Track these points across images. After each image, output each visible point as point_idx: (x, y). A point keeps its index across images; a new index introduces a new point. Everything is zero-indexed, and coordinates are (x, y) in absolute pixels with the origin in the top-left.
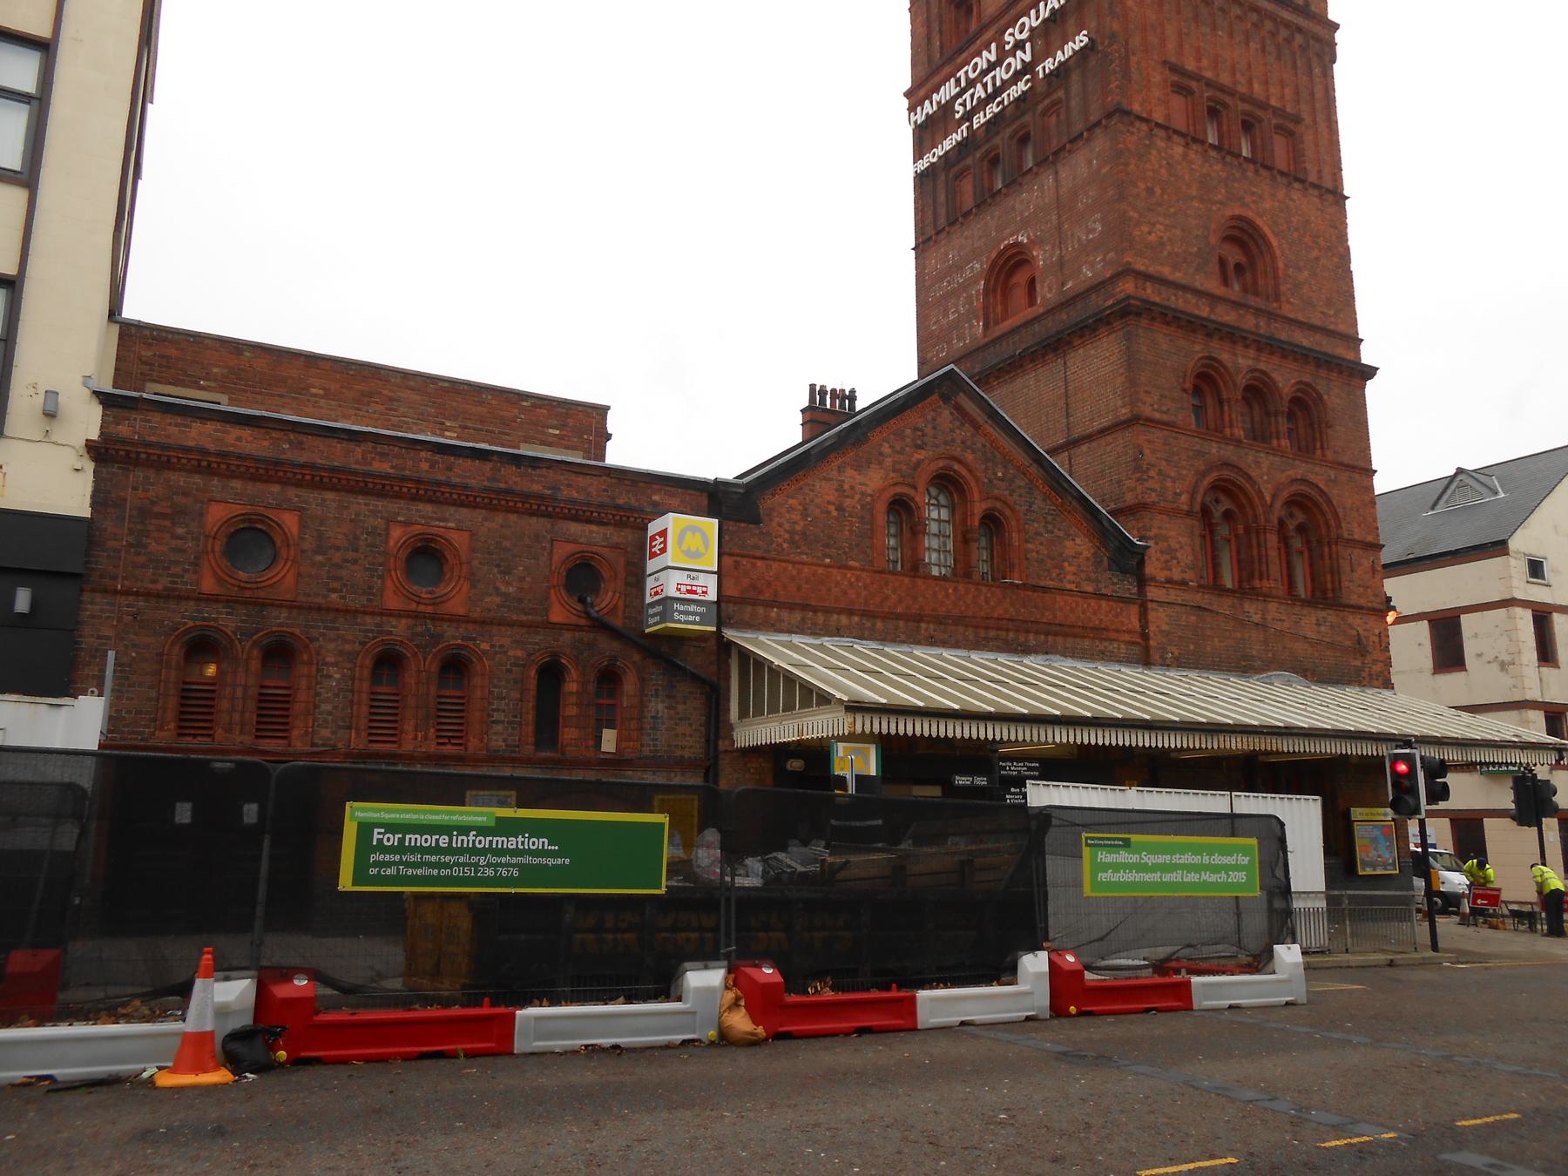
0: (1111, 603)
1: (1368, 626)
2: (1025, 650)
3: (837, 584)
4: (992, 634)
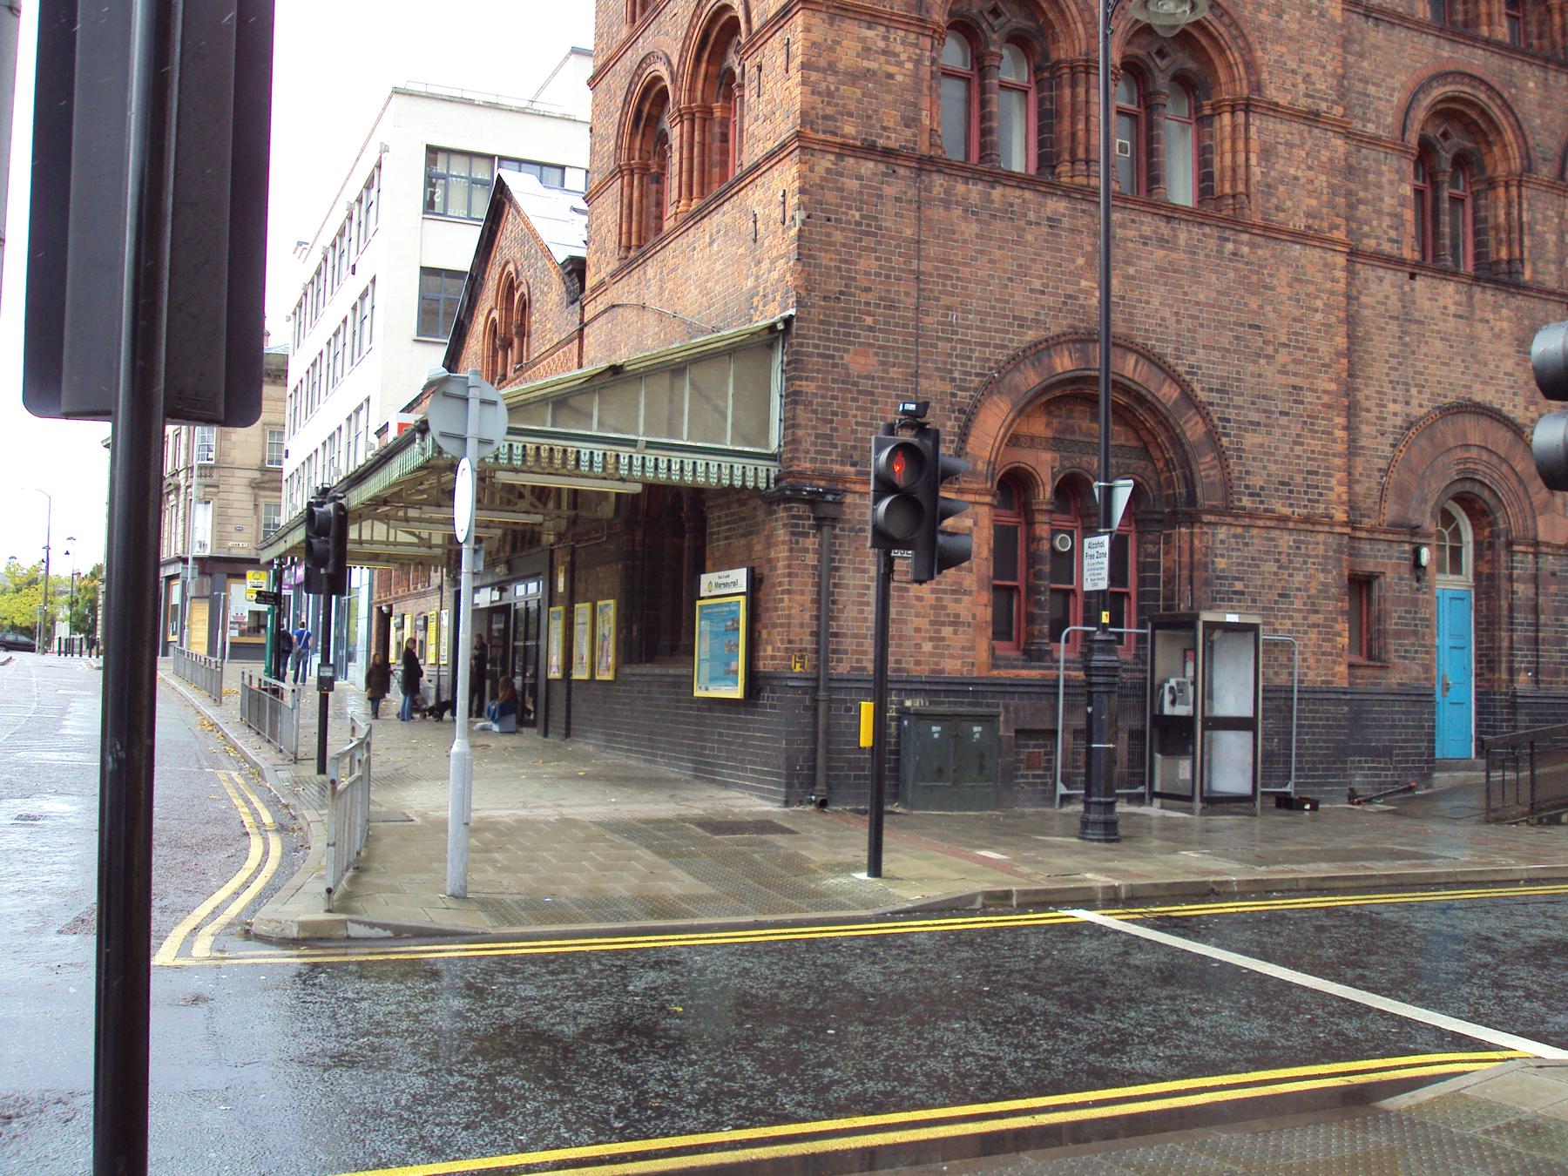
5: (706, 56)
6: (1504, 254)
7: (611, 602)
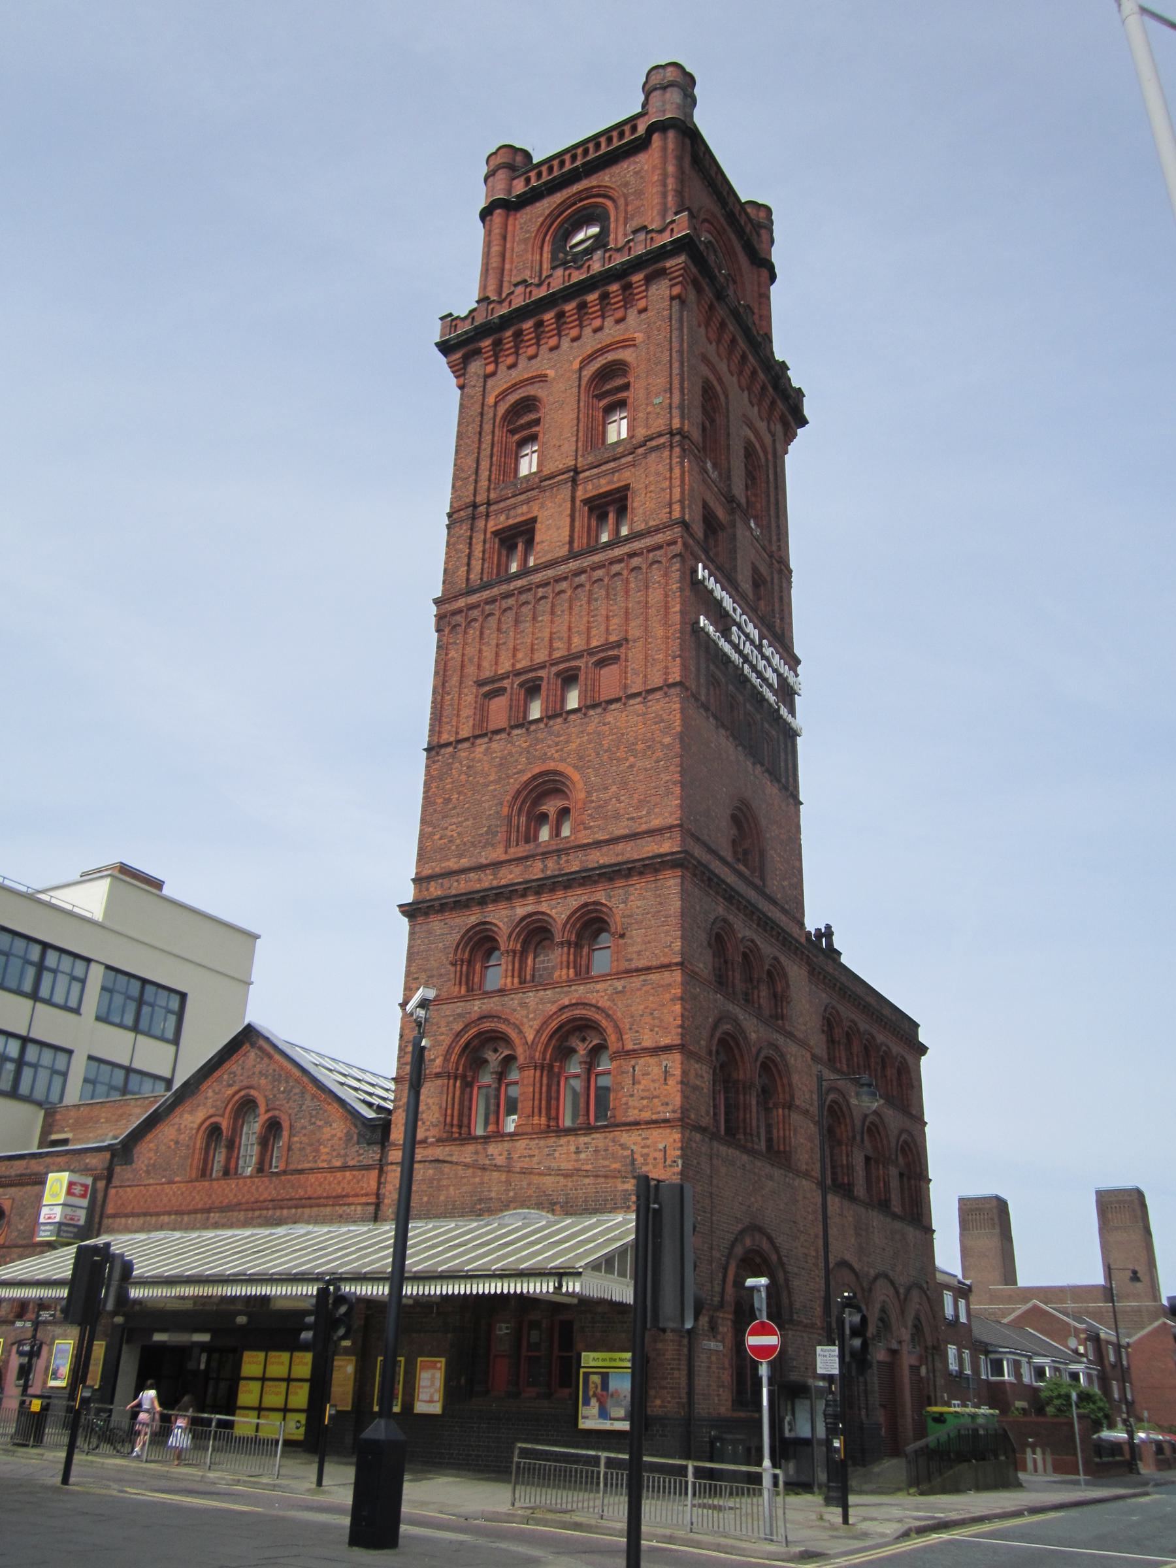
0: (354, 1173)
1: (649, 1142)
2: (279, 1223)
3: (167, 1194)
4: (257, 1213)
5: (557, 1037)
6: (846, 1180)
7: (443, 1360)
